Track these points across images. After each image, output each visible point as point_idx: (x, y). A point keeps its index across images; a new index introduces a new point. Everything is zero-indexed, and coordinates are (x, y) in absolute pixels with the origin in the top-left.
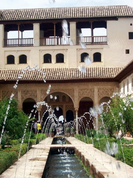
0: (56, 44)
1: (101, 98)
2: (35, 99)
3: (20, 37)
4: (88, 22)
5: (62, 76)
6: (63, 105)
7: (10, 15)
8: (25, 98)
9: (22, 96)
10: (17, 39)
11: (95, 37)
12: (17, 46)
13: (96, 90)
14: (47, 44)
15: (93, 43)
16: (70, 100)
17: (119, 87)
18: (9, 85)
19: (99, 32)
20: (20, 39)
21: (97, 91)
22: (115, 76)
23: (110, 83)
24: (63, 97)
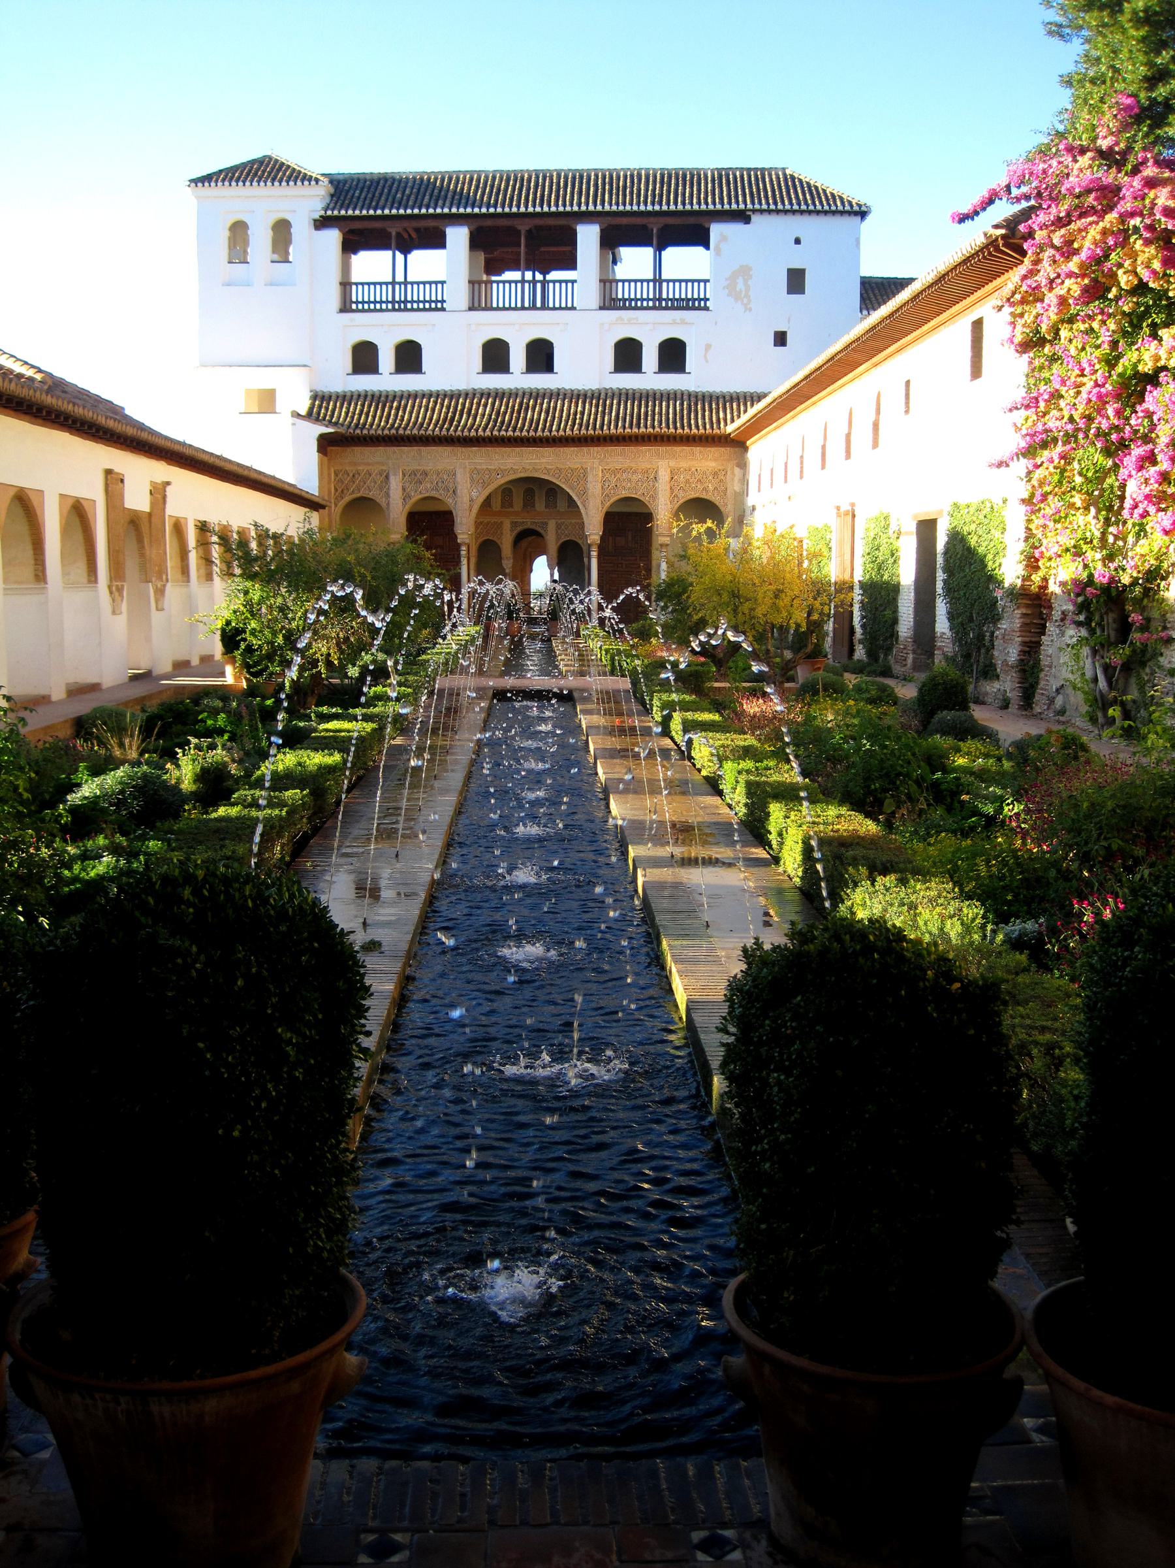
0: (527, 305)
1: (681, 501)
3: (400, 277)
4: (644, 227)
5: (545, 421)
6: (547, 524)
7: (363, 196)
9: (404, 489)
10: (387, 284)
11: (668, 281)
12: (387, 310)
13: (664, 476)
14: (495, 305)
15: (660, 304)
17: (743, 465)
18: (358, 450)
20: (400, 284)
21: (667, 478)
22: (730, 428)
23: (713, 449)
24: (547, 493)
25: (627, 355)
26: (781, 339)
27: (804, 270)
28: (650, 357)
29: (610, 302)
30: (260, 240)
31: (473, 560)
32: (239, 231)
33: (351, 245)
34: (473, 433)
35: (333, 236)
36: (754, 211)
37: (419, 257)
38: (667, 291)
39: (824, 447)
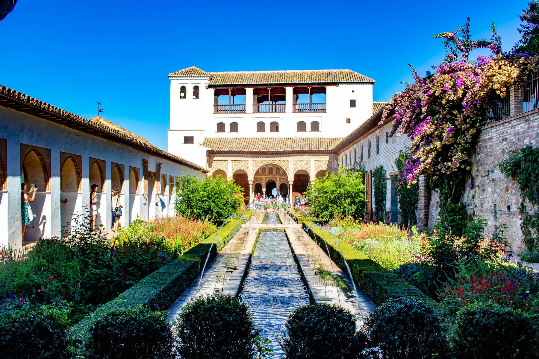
2: (247, 171)
3: (232, 103)
4: (306, 88)
8: (236, 169)
13: (313, 163)
15: (311, 110)
16: (284, 173)
17: (337, 160)
19: (317, 98)
25: (301, 126)
26: (349, 121)
27: (355, 100)
28: (308, 127)
29: (295, 111)
31: (254, 189)
33: (217, 94)
35: (212, 91)
36: (340, 83)
37: (237, 97)
38: (314, 107)
39: (362, 153)
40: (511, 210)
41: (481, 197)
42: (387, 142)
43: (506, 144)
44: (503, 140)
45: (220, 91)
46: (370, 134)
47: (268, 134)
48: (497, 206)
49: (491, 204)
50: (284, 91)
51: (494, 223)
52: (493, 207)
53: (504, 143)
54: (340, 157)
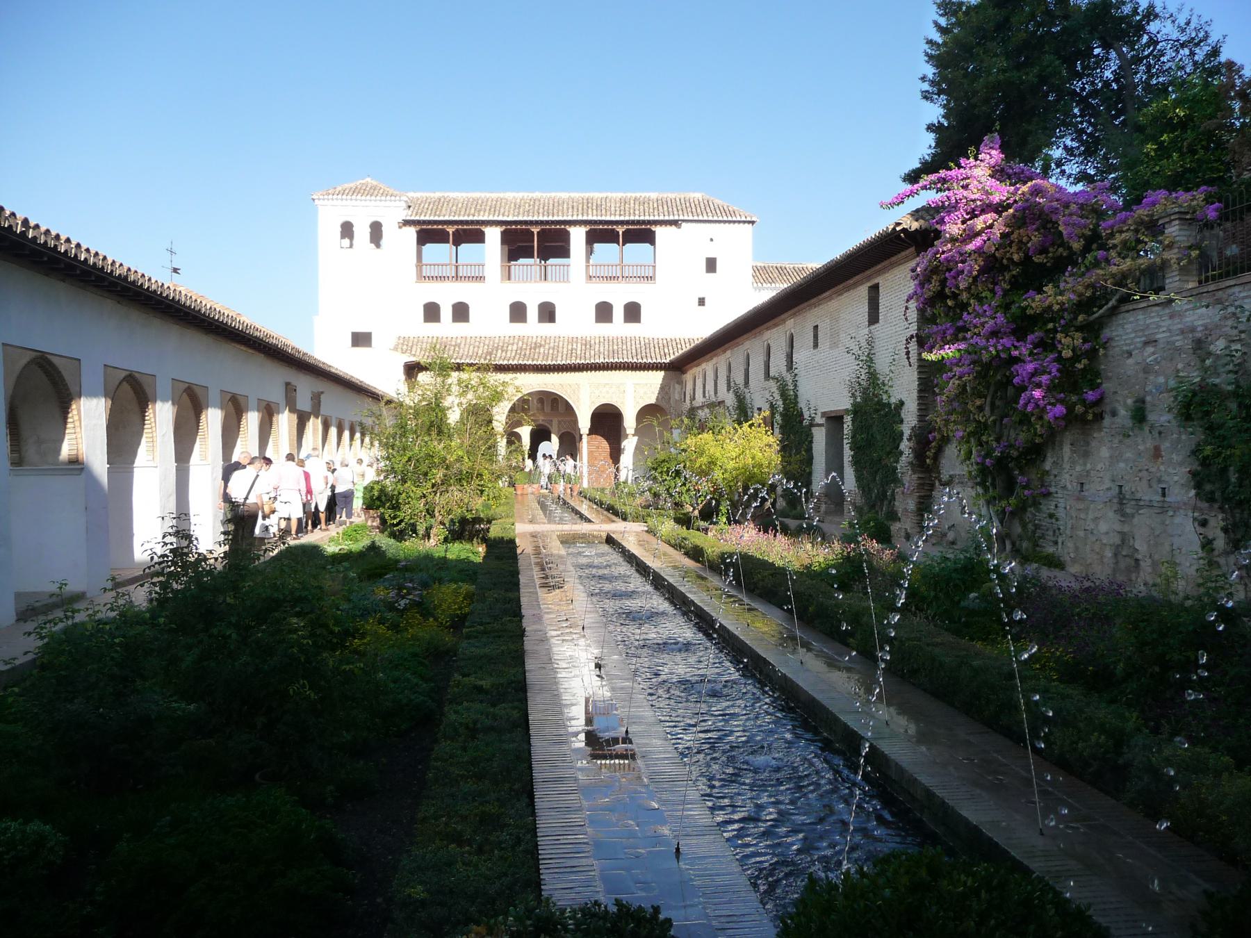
16: (569, 410)
17: (680, 382)
19: (636, 251)
25: (604, 312)
28: (618, 313)
30: (362, 233)
32: (347, 230)
34: (505, 362)
40: (1167, 499)
41: (1078, 468)
42: (816, 345)
43: (1154, 353)
44: (1146, 343)
45: (429, 234)
46: (768, 329)
47: (532, 327)
48: (1126, 489)
49: (1108, 484)
50: (565, 236)
51: (1118, 527)
52: (1116, 490)
53: (1150, 349)
54: (688, 377)
